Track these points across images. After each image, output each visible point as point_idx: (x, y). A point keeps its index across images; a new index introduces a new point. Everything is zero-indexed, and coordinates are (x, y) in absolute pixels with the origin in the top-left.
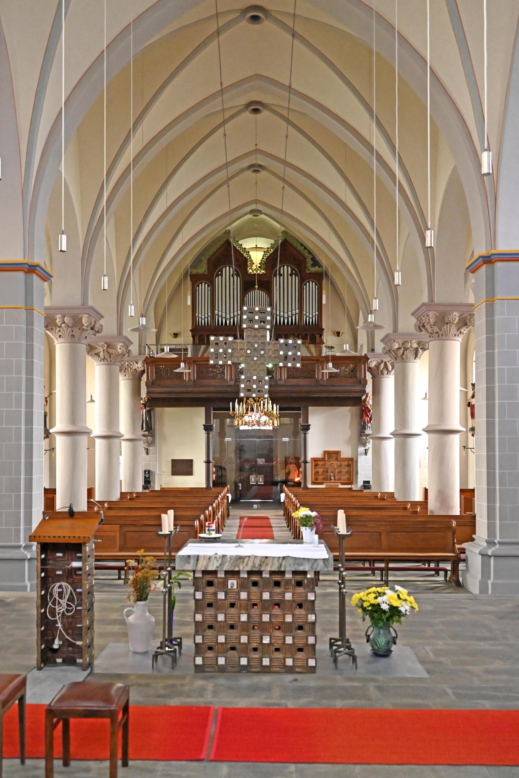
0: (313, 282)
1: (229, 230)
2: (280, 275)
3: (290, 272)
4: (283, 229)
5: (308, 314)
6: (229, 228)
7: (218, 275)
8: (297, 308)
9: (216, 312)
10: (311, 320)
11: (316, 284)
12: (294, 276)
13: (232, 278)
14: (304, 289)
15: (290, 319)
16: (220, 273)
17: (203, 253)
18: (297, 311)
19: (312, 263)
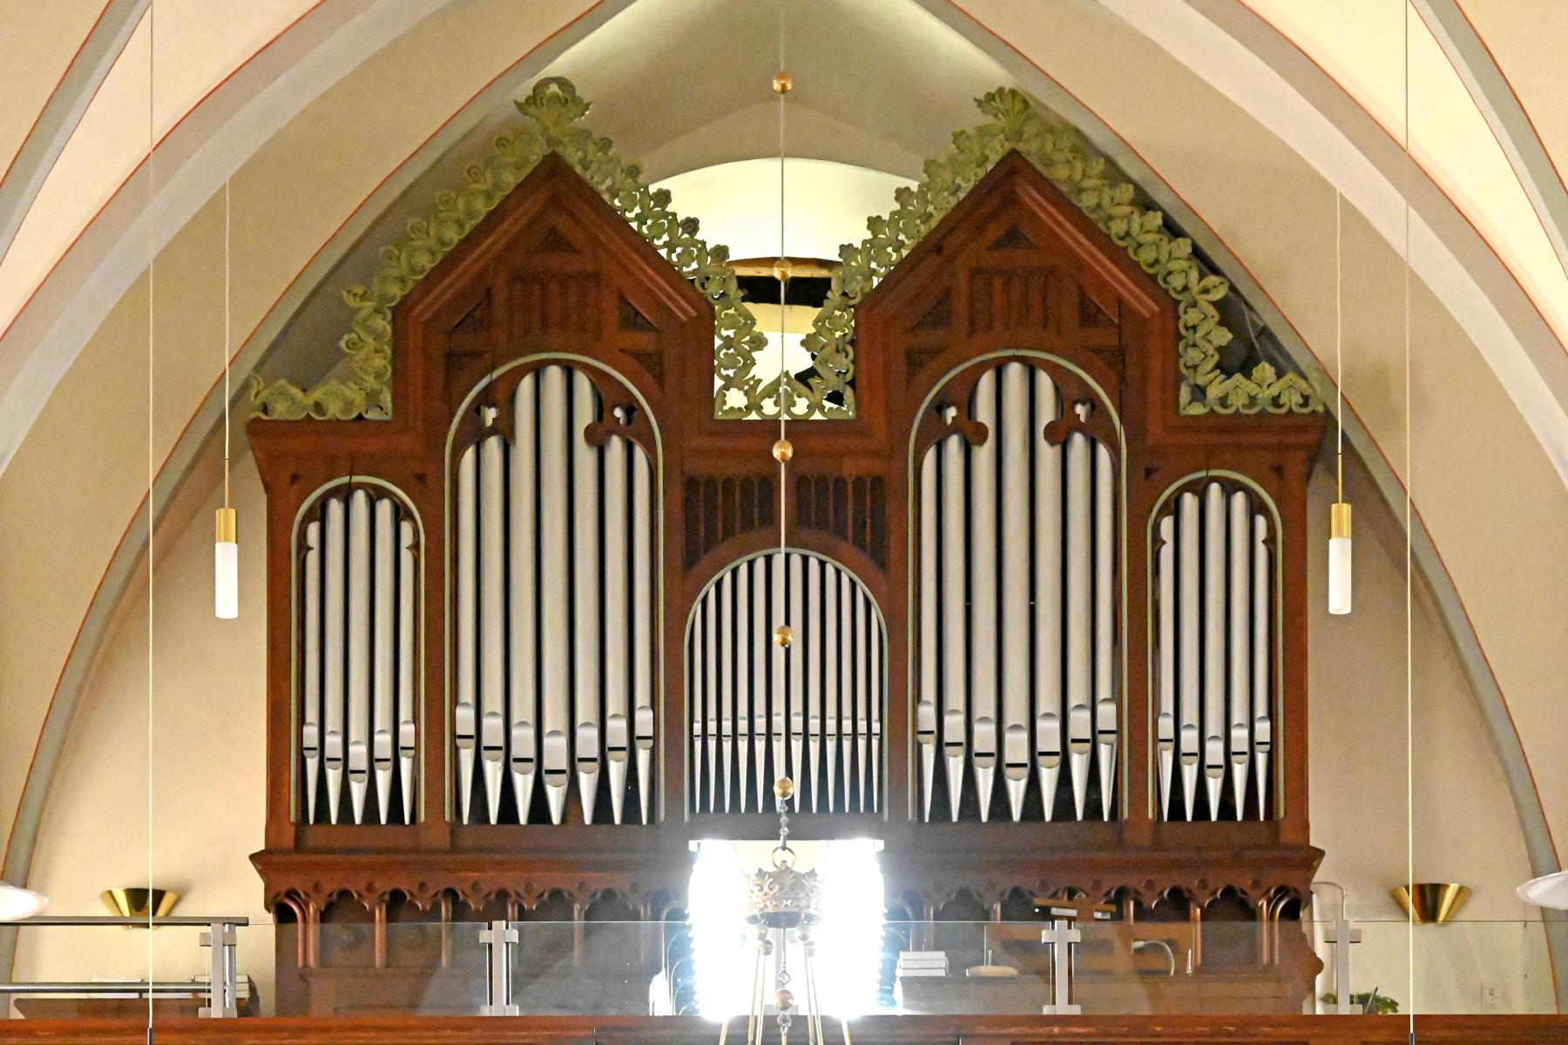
0: (1229, 488)
1: (561, 82)
2: (972, 436)
3: (1047, 414)
4: (992, 72)
5: (1189, 740)
6: (559, 66)
7: (475, 435)
8: (1104, 690)
9: (465, 718)
10: (1214, 787)
11: (1256, 507)
12: (1078, 440)
13: (585, 457)
14: (1158, 541)
15: (1048, 779)
16: (490, 415)
17: (355, 261)
18: (1107, 714)
19: (1224, 337)
